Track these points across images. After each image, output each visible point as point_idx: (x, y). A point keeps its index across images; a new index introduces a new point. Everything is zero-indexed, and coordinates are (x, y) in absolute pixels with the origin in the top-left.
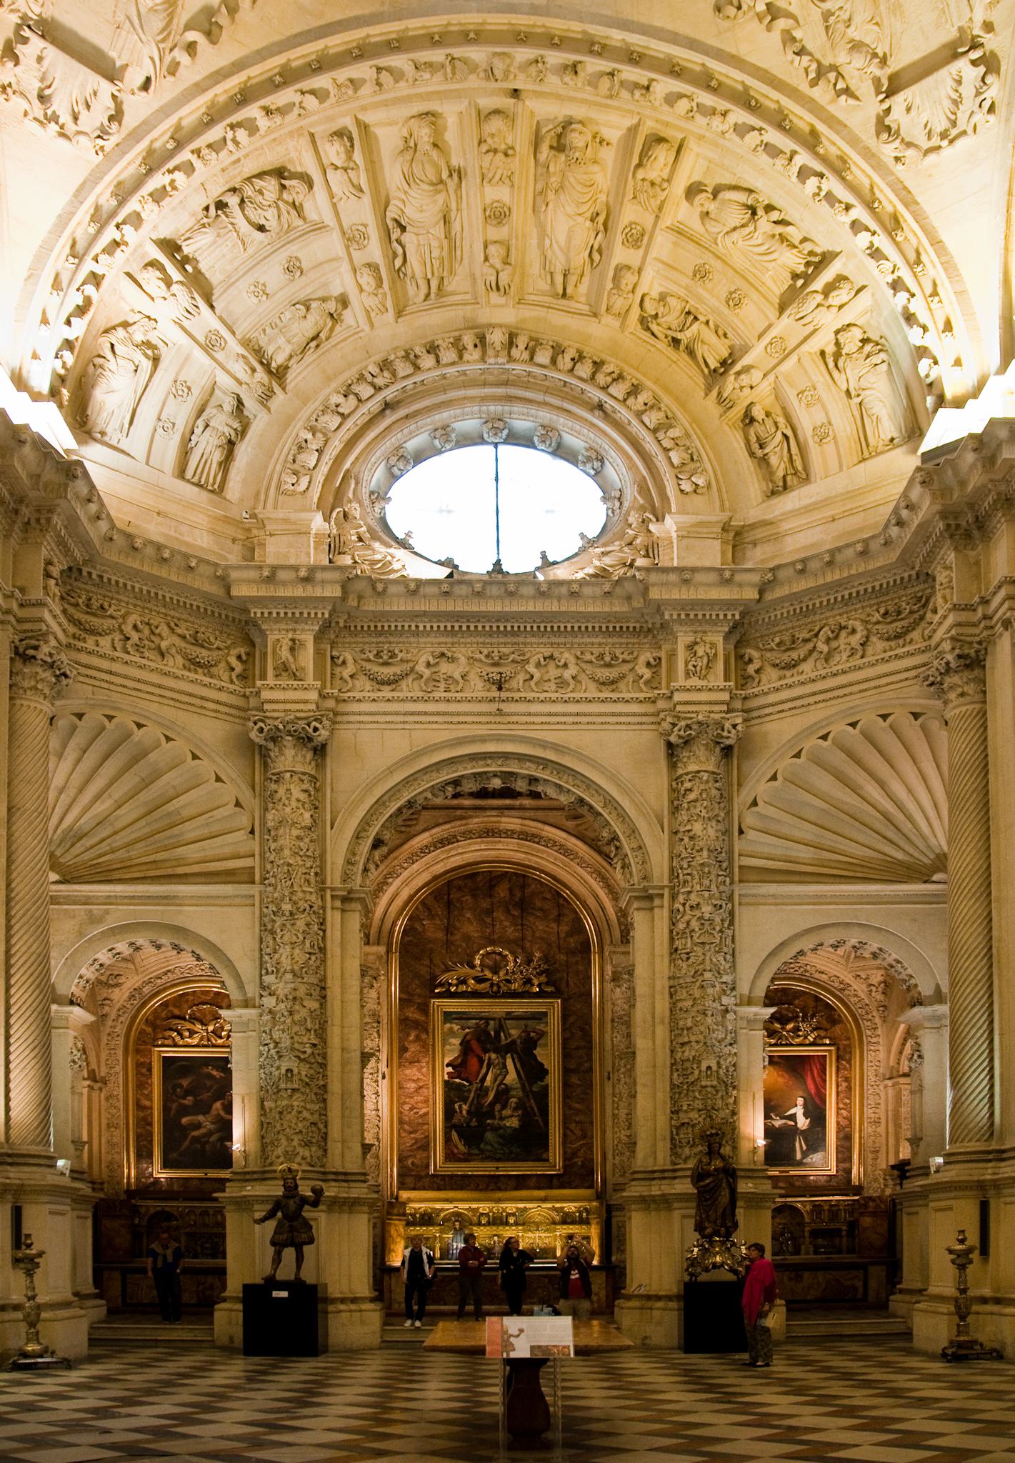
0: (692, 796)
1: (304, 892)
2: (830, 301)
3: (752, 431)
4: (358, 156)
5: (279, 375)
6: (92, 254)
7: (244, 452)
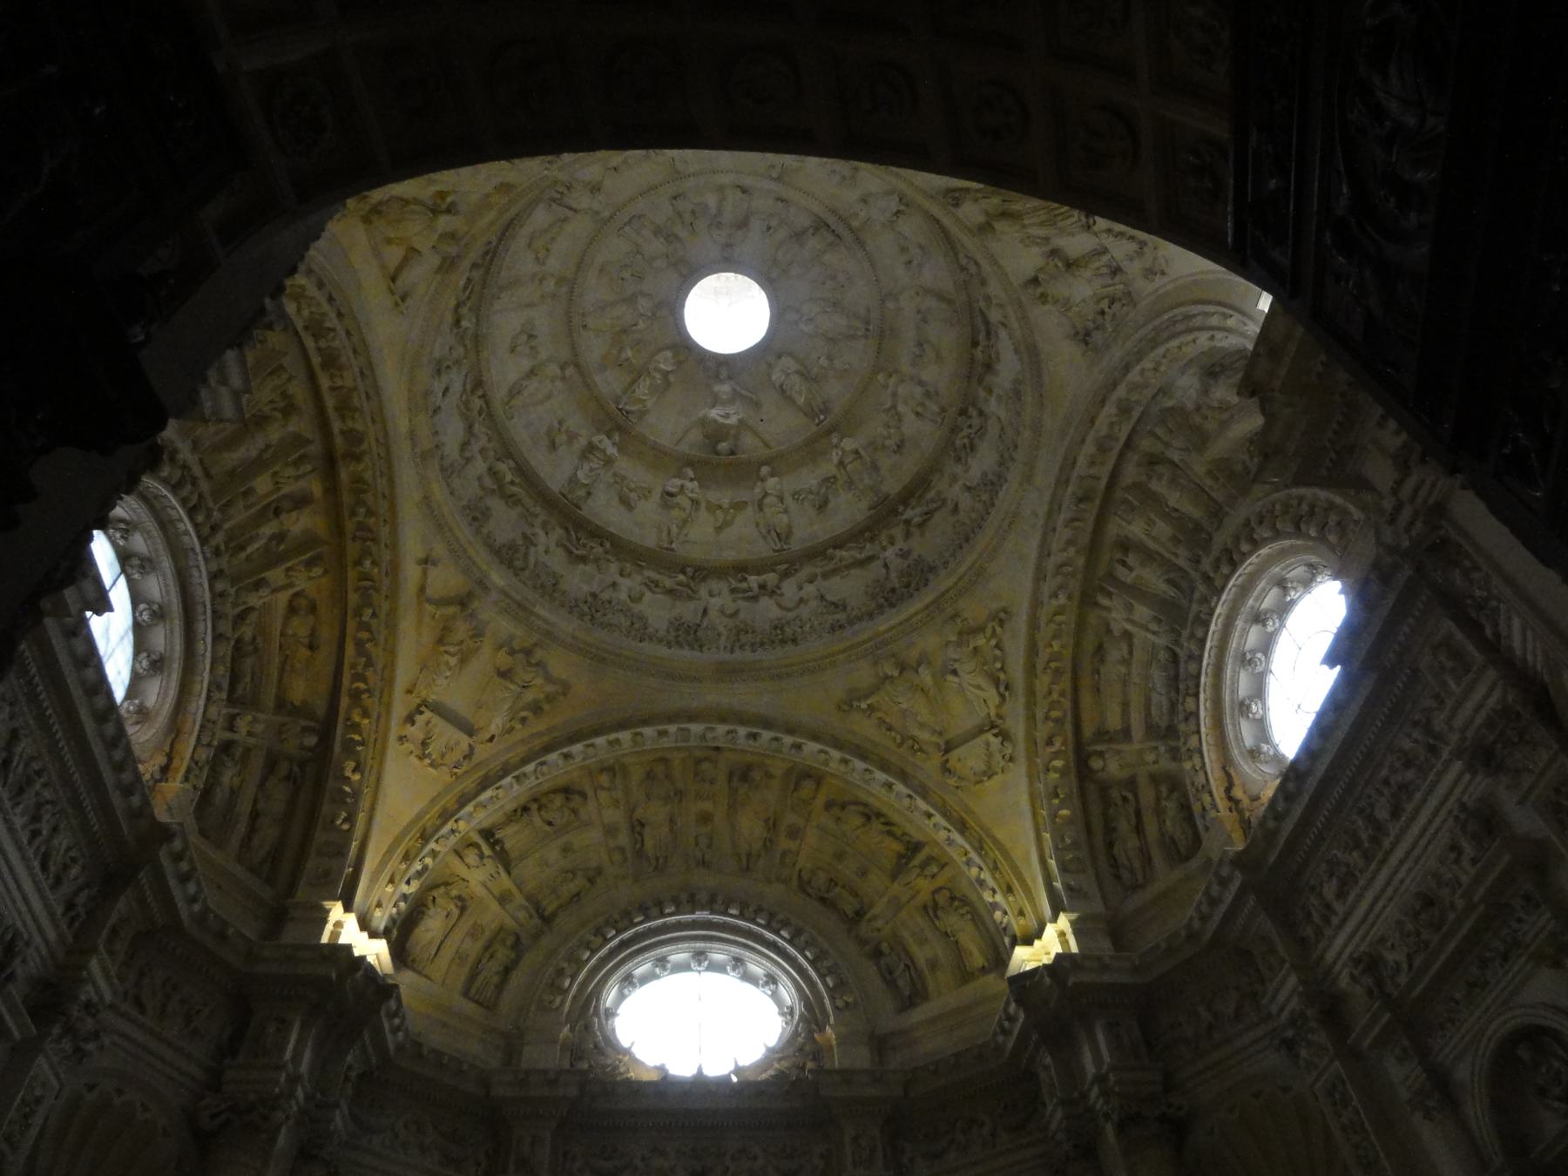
2: (926, 873)
3: (882, 962)
4: (618, 781)
5: (547, 920)
6: (436, 837)
7: (517, 979)
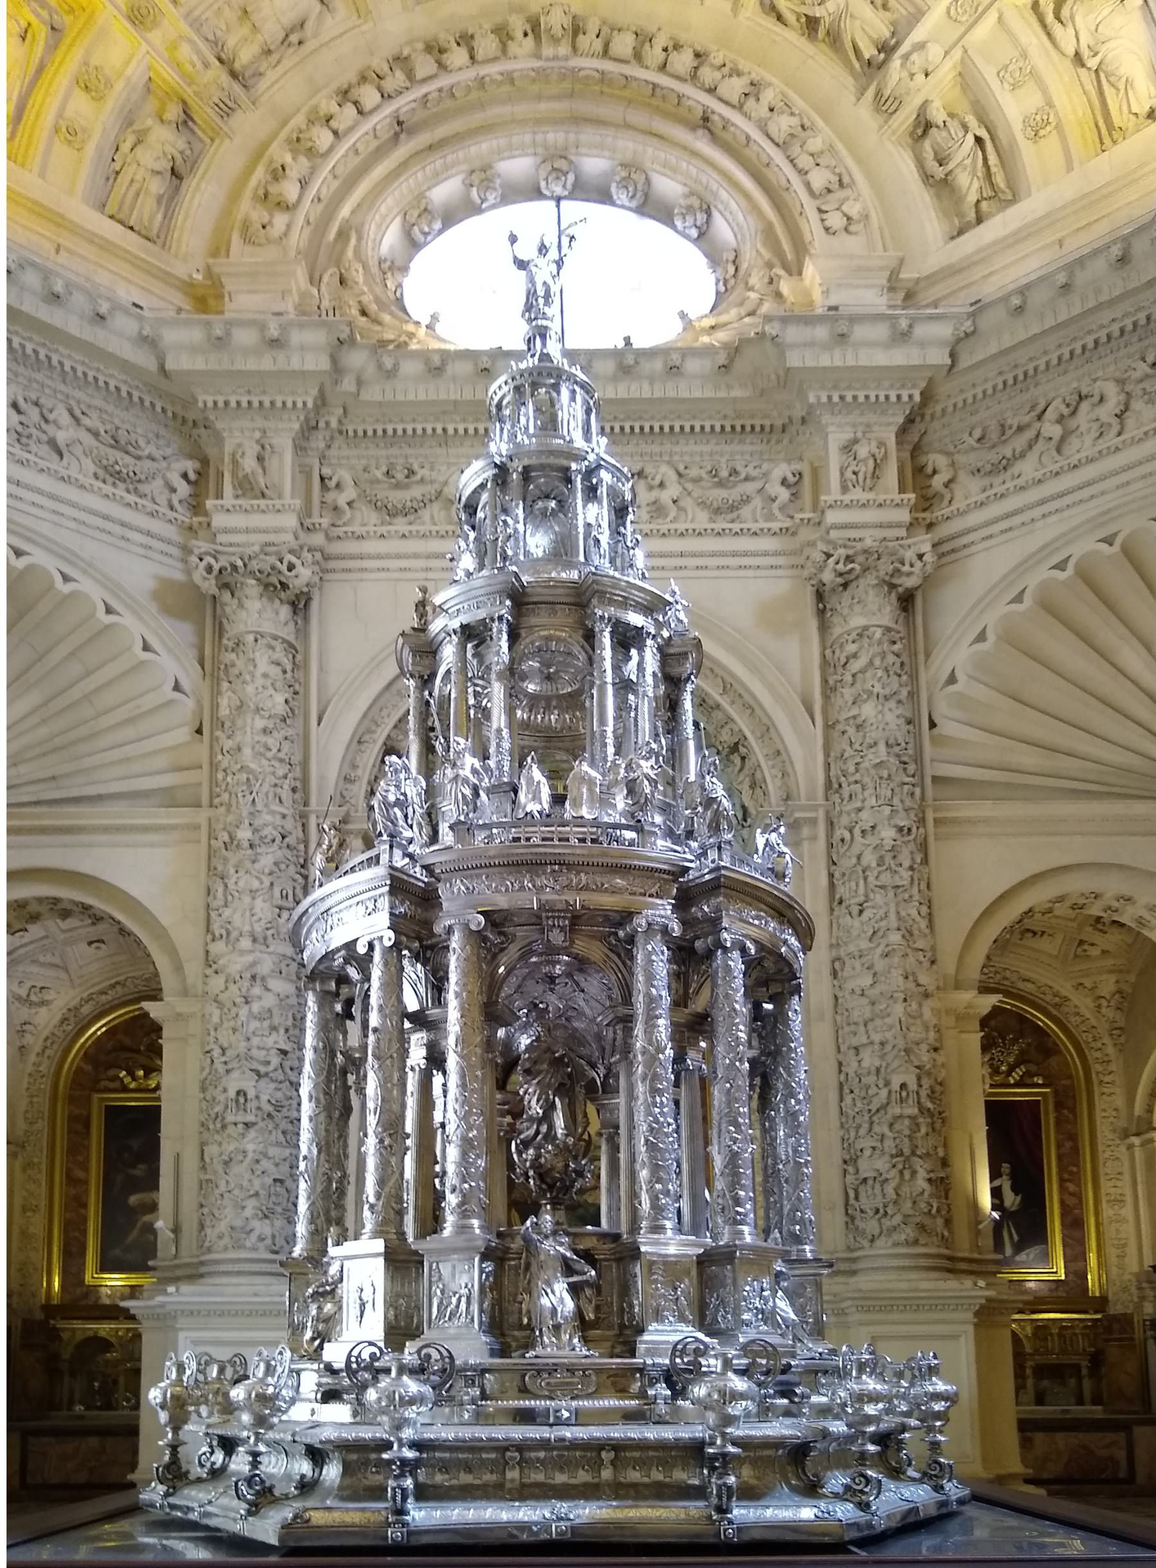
0: (855, 666)
1: (273, 813)
